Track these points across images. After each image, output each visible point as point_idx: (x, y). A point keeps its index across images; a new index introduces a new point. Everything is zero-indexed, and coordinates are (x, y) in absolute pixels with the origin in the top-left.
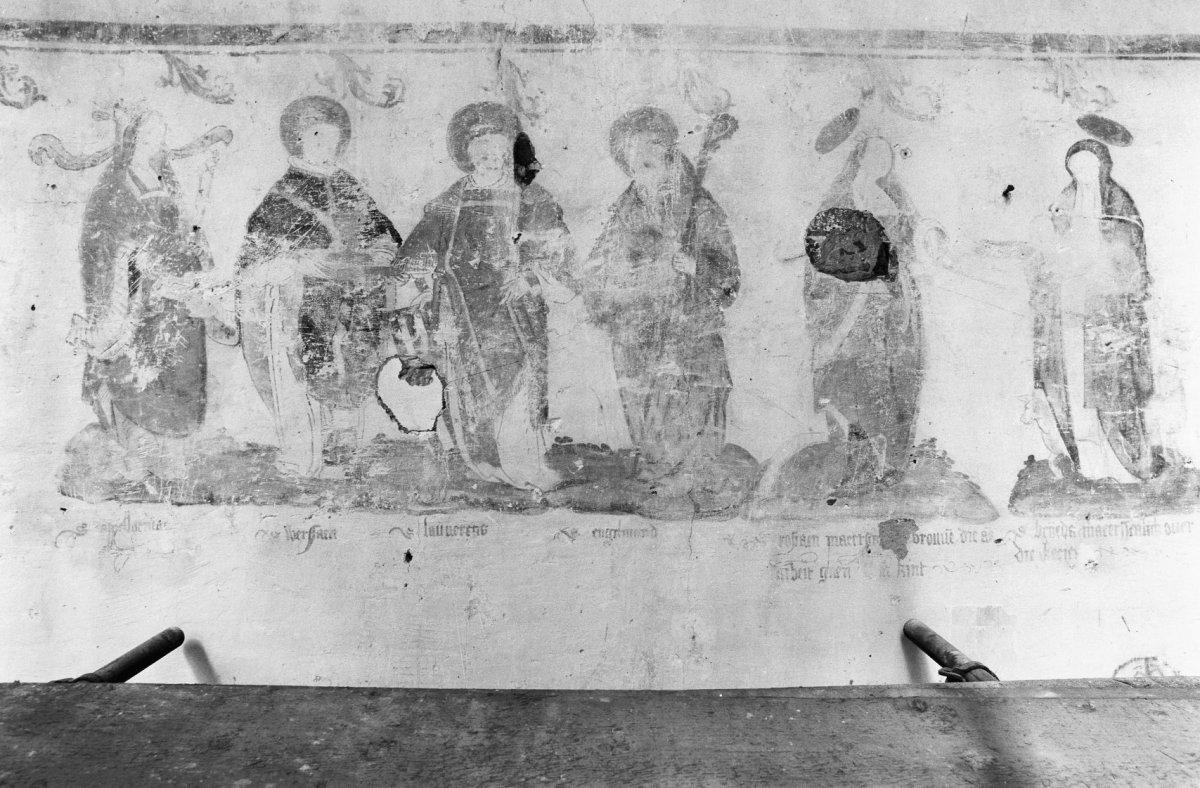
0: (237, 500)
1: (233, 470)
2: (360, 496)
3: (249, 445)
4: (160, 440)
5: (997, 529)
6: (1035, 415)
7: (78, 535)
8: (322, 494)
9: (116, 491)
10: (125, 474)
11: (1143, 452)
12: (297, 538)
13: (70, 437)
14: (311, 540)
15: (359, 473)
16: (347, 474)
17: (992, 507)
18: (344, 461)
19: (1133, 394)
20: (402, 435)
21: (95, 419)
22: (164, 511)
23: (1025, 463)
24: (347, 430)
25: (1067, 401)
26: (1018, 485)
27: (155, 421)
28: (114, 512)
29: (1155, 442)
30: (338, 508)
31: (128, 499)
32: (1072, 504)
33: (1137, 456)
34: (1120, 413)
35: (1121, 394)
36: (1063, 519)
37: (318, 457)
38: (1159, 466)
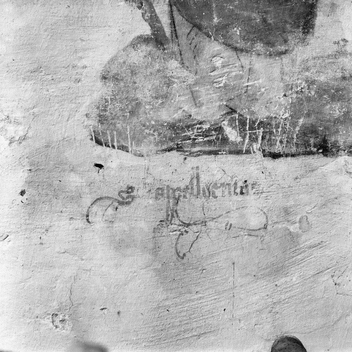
4: (245, 60)
7: (121, 203)
9: (178, 137)
10: (193, 111)
13: (107, 58)
21: (146, 30)
22: (250, 166)
27: (237, 31)
28: (174, 169)
31: (197, 149)
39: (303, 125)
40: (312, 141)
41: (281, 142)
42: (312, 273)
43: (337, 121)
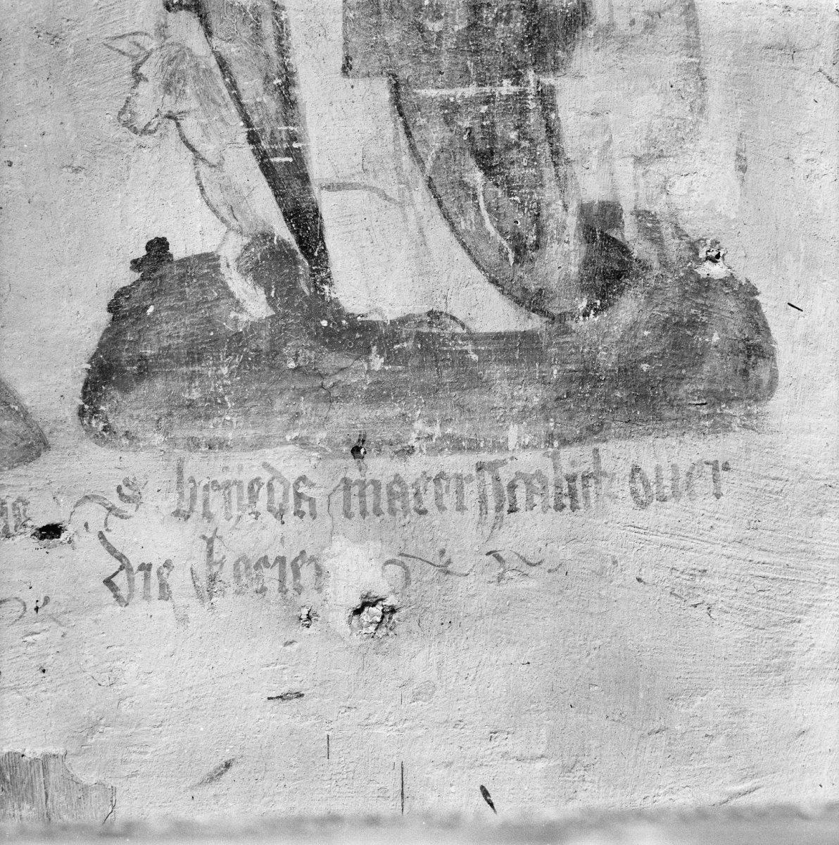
5: (38, 491)
6: (169, 104)
11: (551, 226)
17: (23, 415)
19: (518, 25)
23: (136, 265)
25: (282, 52)
26: (112, 338)
29: (592, 189)
32: (304, 406)
33: (532, 238)
34: (471, 91)
35: (473, 26)
36: (269, 455)
38: (610, 269)
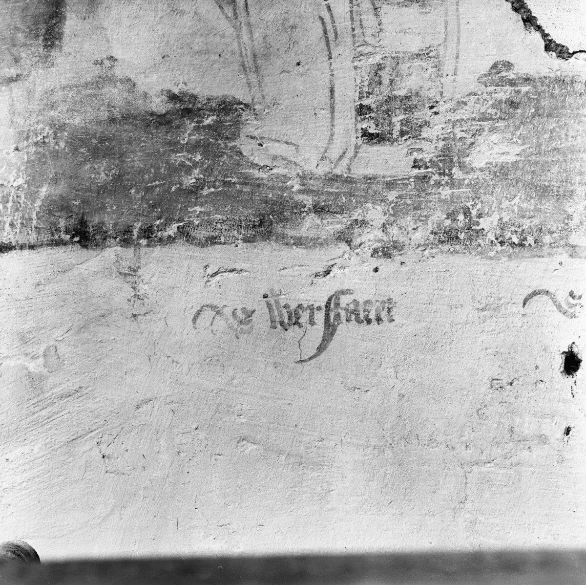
0: (147, 233)
1: (136, 160)
2: (452, 216)
3: (173, 98)
8: (357, 215)
12: (297, 323)
14: (330, 329)
15: (448, 159)
16: (416, 165)
18: (411, 131)
20: (551, 64)
24: (418, 55)
30: (397, 246)
37: (347, 125)
39: (47, 197)
40: (62, 223)
41: (12, 225)
42: (64, 439)
43: (102, 190)
